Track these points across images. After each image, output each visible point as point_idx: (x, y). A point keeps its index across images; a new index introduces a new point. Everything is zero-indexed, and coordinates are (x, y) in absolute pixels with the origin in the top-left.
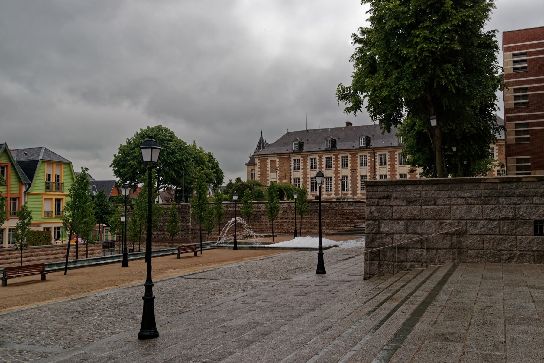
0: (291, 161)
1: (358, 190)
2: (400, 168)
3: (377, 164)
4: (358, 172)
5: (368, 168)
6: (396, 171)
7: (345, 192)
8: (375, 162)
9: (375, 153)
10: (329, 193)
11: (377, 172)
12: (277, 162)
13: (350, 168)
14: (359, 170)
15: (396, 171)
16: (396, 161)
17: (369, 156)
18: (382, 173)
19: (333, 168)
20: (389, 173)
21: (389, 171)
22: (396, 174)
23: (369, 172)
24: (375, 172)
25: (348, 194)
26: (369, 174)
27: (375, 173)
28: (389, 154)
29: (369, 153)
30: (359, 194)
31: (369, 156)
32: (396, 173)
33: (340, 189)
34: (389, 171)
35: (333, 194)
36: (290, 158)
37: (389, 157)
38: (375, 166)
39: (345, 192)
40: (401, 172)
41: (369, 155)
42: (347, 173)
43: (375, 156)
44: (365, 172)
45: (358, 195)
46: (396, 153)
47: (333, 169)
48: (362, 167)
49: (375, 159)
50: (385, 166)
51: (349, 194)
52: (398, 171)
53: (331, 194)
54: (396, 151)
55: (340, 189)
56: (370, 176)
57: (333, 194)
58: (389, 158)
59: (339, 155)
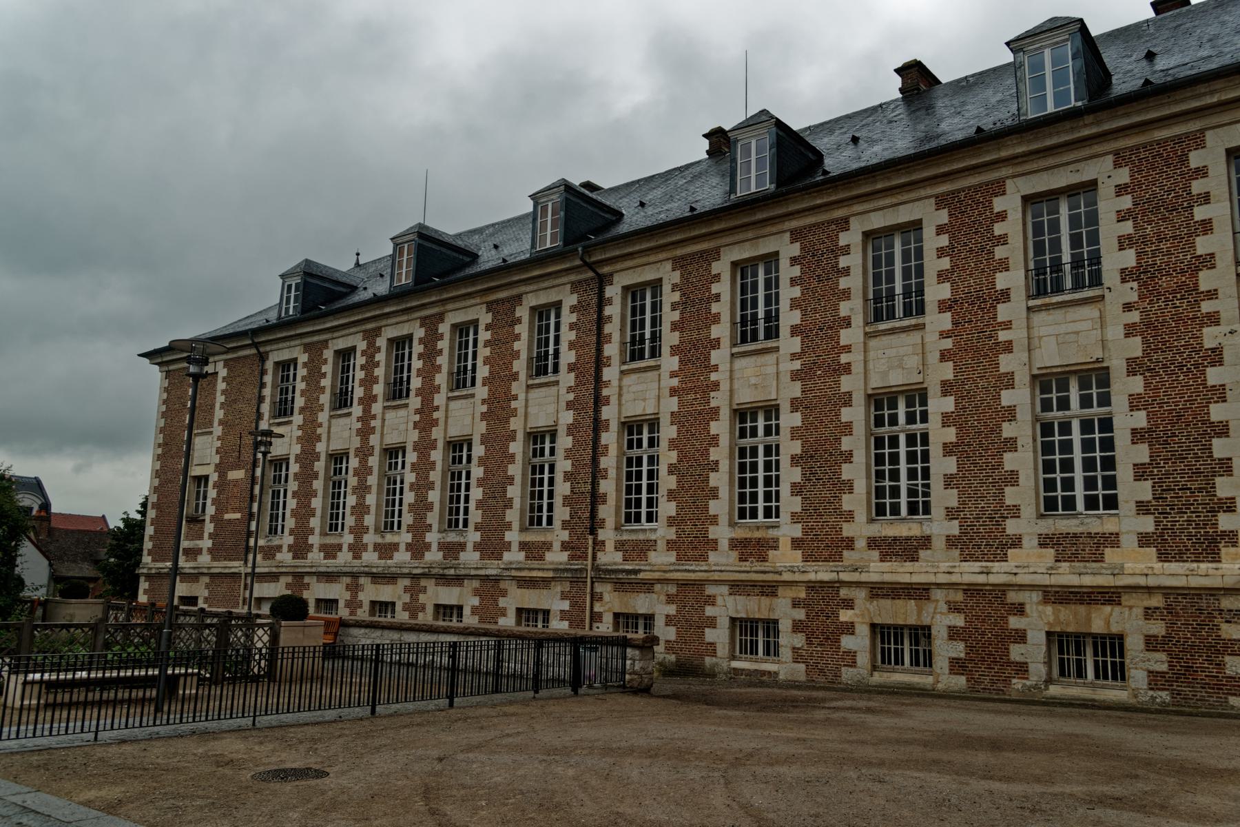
0: (263, 372)
1: (508, 526)
2: (740, 363)
3: (612, 350)
4: (514, 413)
5: (567, 379)
6: (716, 386)
7: (452, 537)
8: (601, 339)
9: (603, 281)
10: (389, 538)
11: (607, 401)
12: (220, 380)
13: (481, 392)
14: (522, 396)
15: (716, 386)
16: (716, 319)
17: (573, 309)
18: (634, 409)
19: (412, 393)
20: (673, 404)
21: (673, 392)
22: (714, 413)
23: (570, 405)
24: (599, 401)
25: (462, 546)
26: (568, 417)
27: (597, 411)
28: (676, 277)
29: (575, 286)
30: (515, 547)
31: (573, 309)
32: (719, 400)
33: (433, 518)
34: (673, 392)
35: (402, 547)
36: (263, 358)
37: (676, 297)
38: (600, 362)
39: (452, 537)
40: (745, 396)
41: (573, 300)
42: (468, 420)
43: (602, 302)
44: (551, 408)
45: (507, 556)
46: (716, 267)
47: (415, 402)
48: (542, 379)
49: (601, 321)
50: (652, 362)
51: (470, 546)
52: (724, 386)
53: (395, 547)
54: (715, 254)
55: (433, 518)
56: (571, 430)
57: (402, 547)
58: (674, 307)
59: (441, 317)
